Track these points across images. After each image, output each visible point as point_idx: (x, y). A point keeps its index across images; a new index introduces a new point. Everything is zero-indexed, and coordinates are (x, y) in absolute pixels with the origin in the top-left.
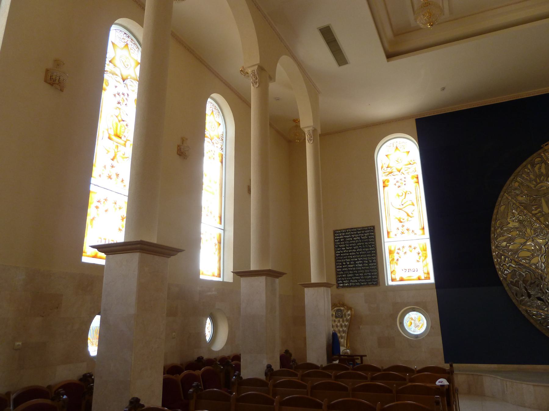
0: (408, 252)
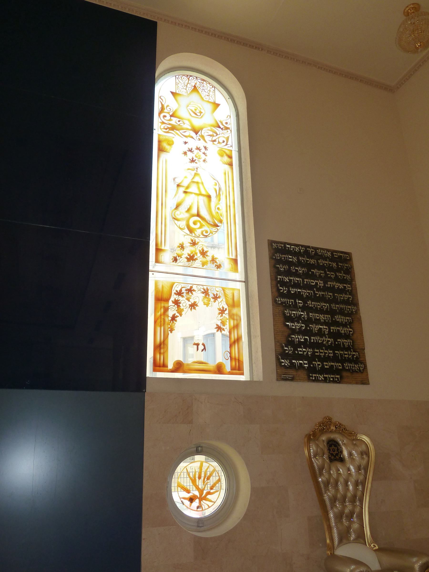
0: (200, 304)
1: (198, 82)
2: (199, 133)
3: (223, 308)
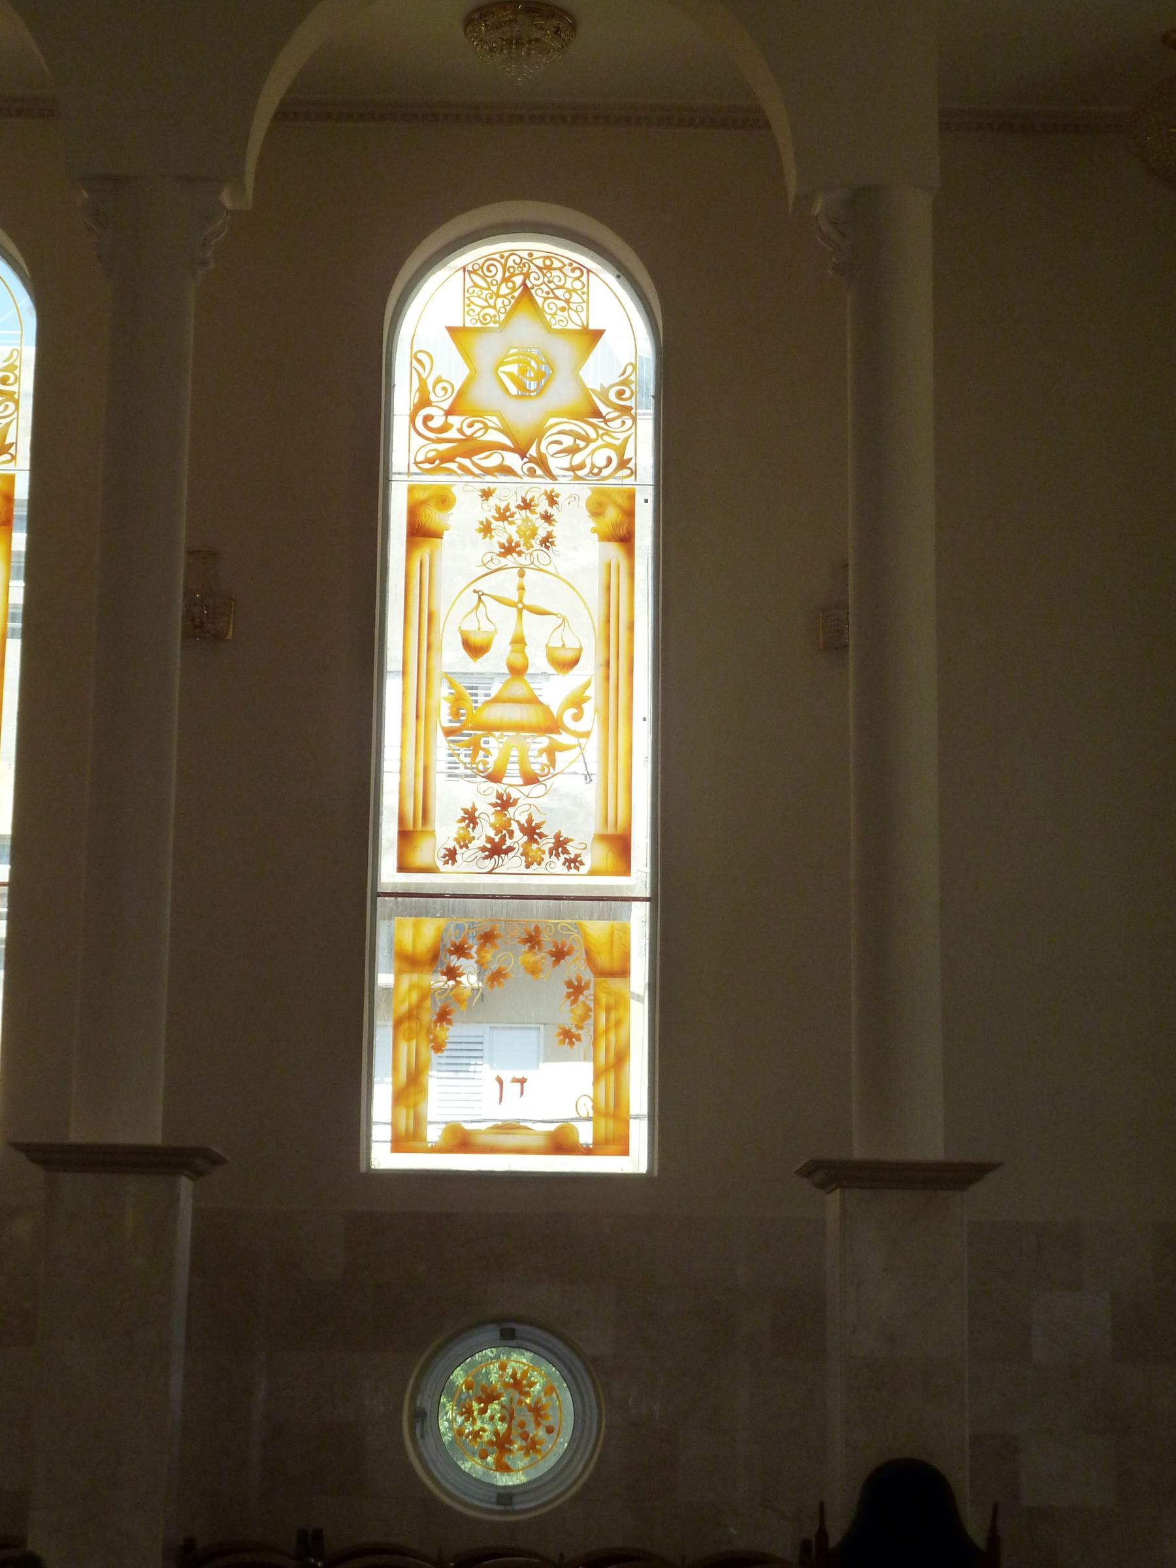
1: (533, 268)
2: (532, 451)
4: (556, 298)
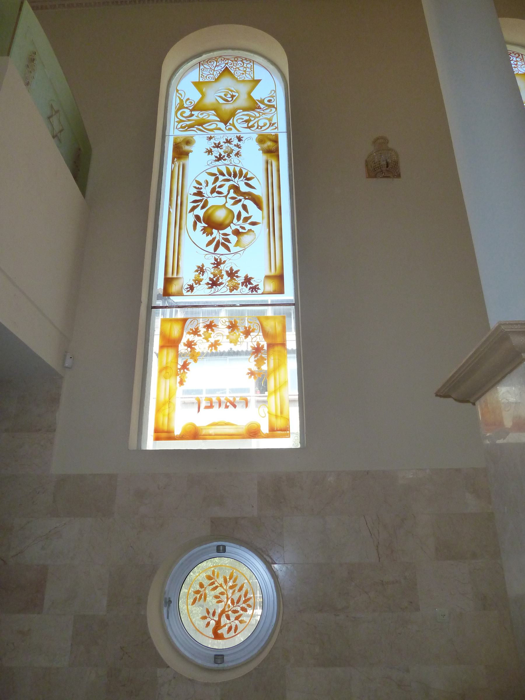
2: (231, 122)
3: (258, 344)
4: (239, 70)
